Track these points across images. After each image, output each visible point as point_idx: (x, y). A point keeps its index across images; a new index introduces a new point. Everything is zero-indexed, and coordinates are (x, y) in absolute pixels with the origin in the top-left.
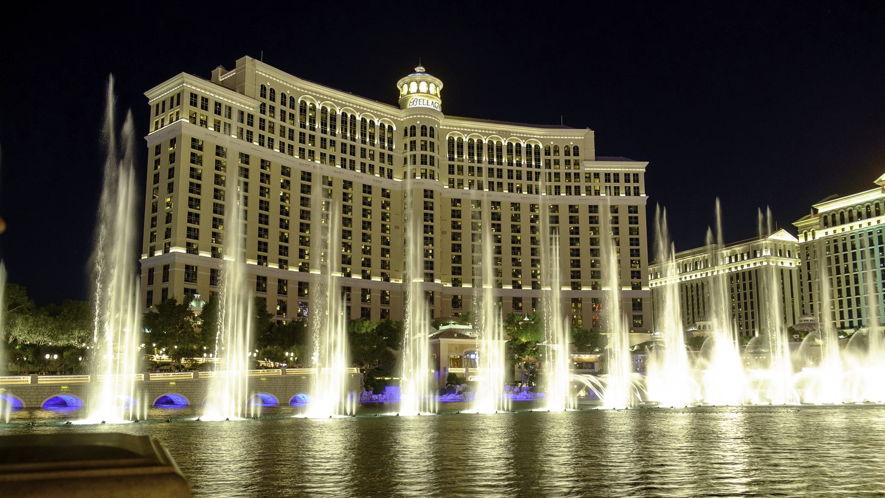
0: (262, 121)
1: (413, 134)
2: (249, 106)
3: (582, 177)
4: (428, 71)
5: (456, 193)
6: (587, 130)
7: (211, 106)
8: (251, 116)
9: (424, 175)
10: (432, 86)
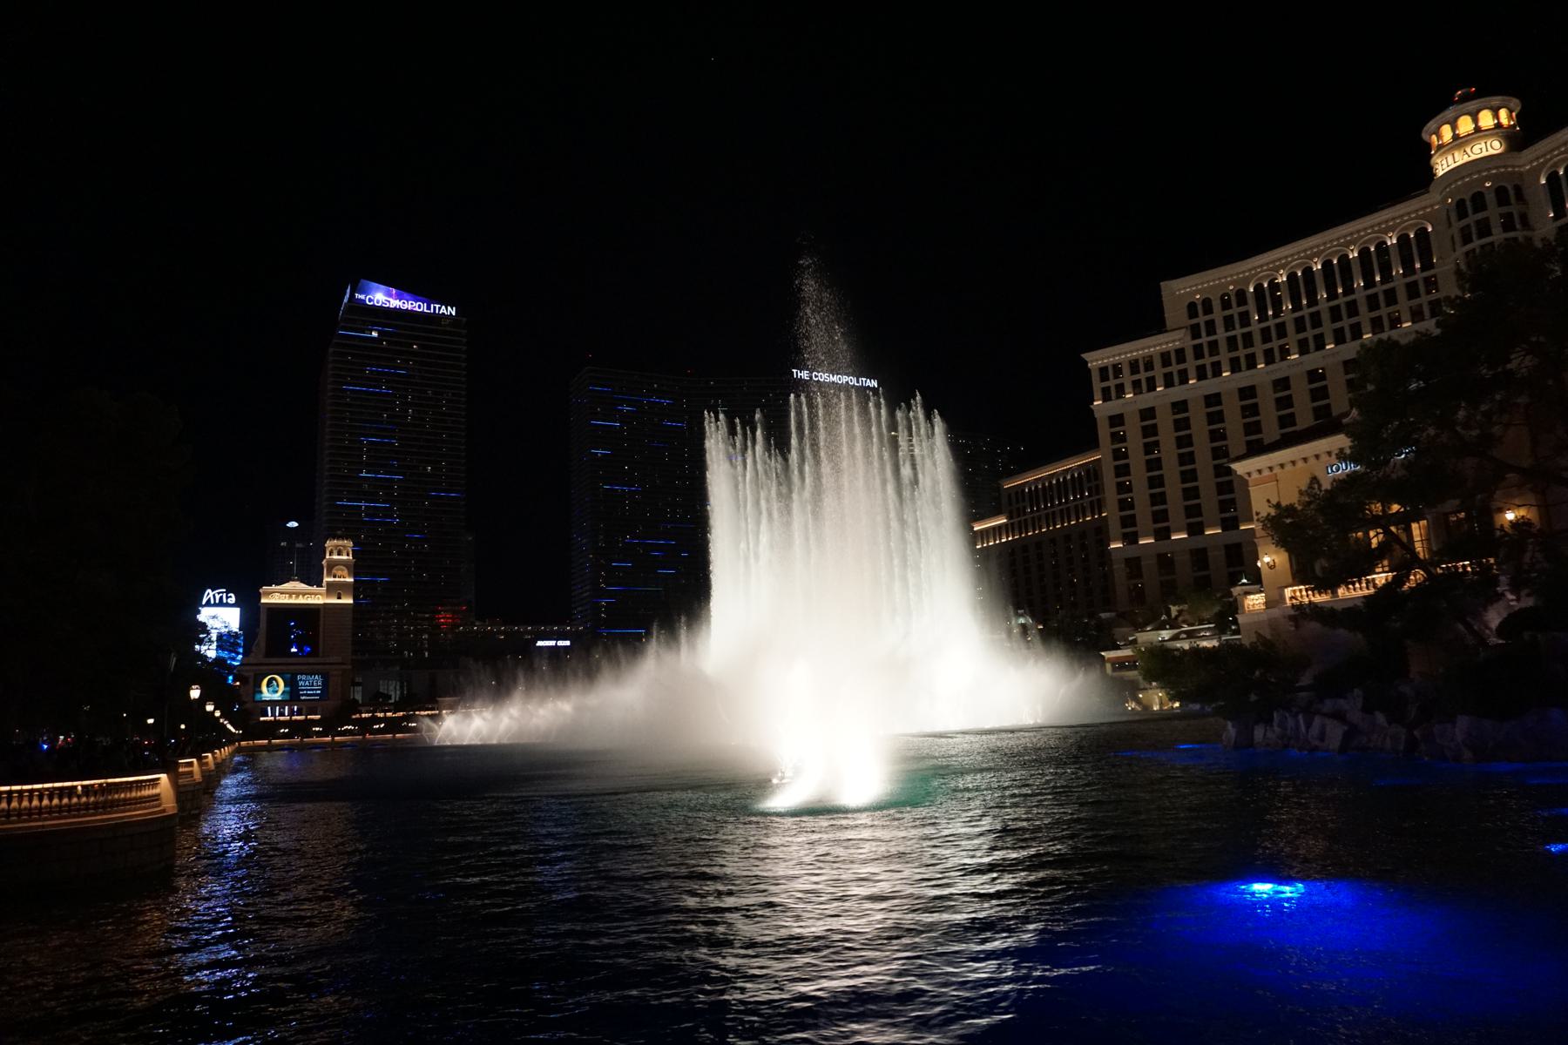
8: (1180, 353)
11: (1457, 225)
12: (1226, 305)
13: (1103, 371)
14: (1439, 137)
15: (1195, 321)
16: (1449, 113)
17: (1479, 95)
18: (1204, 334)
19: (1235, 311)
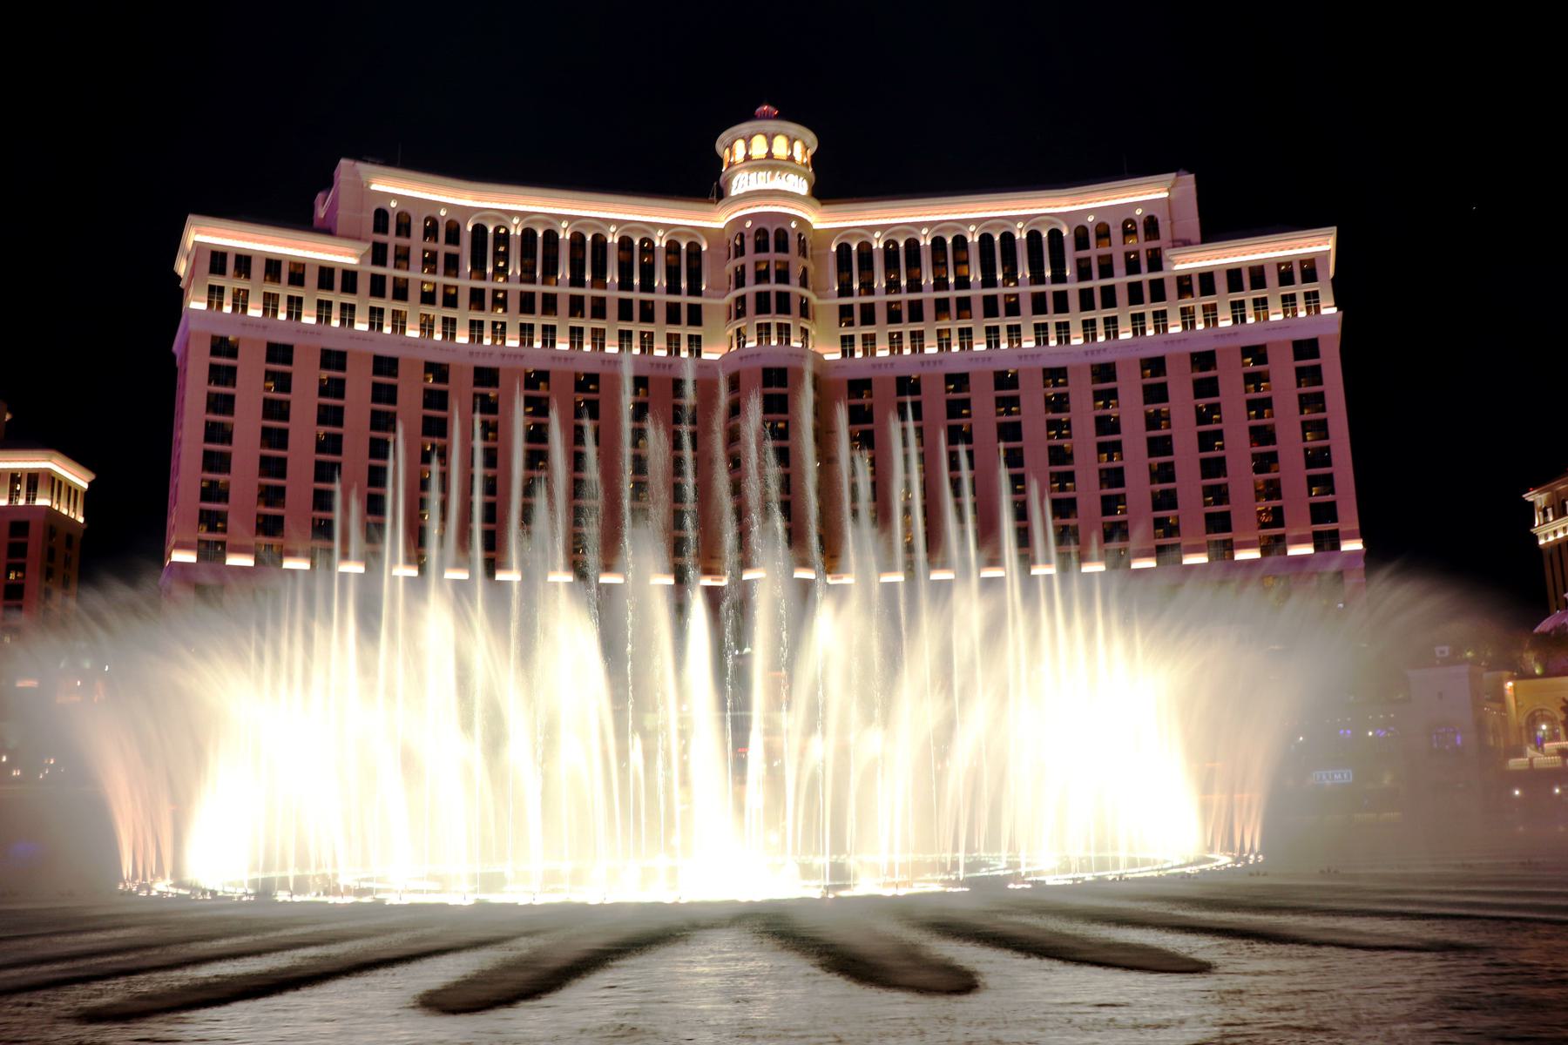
1: (740, 251)
3: (1171, 290)
6: (1172, 176)
7: (258, 269)
8: (350, 280)
11: (750, 259)
12: (431, 231)
13: (218, 261)
14: (748, 147)
15: (381, 238)
17: (779, 117)
19: (442, 248)
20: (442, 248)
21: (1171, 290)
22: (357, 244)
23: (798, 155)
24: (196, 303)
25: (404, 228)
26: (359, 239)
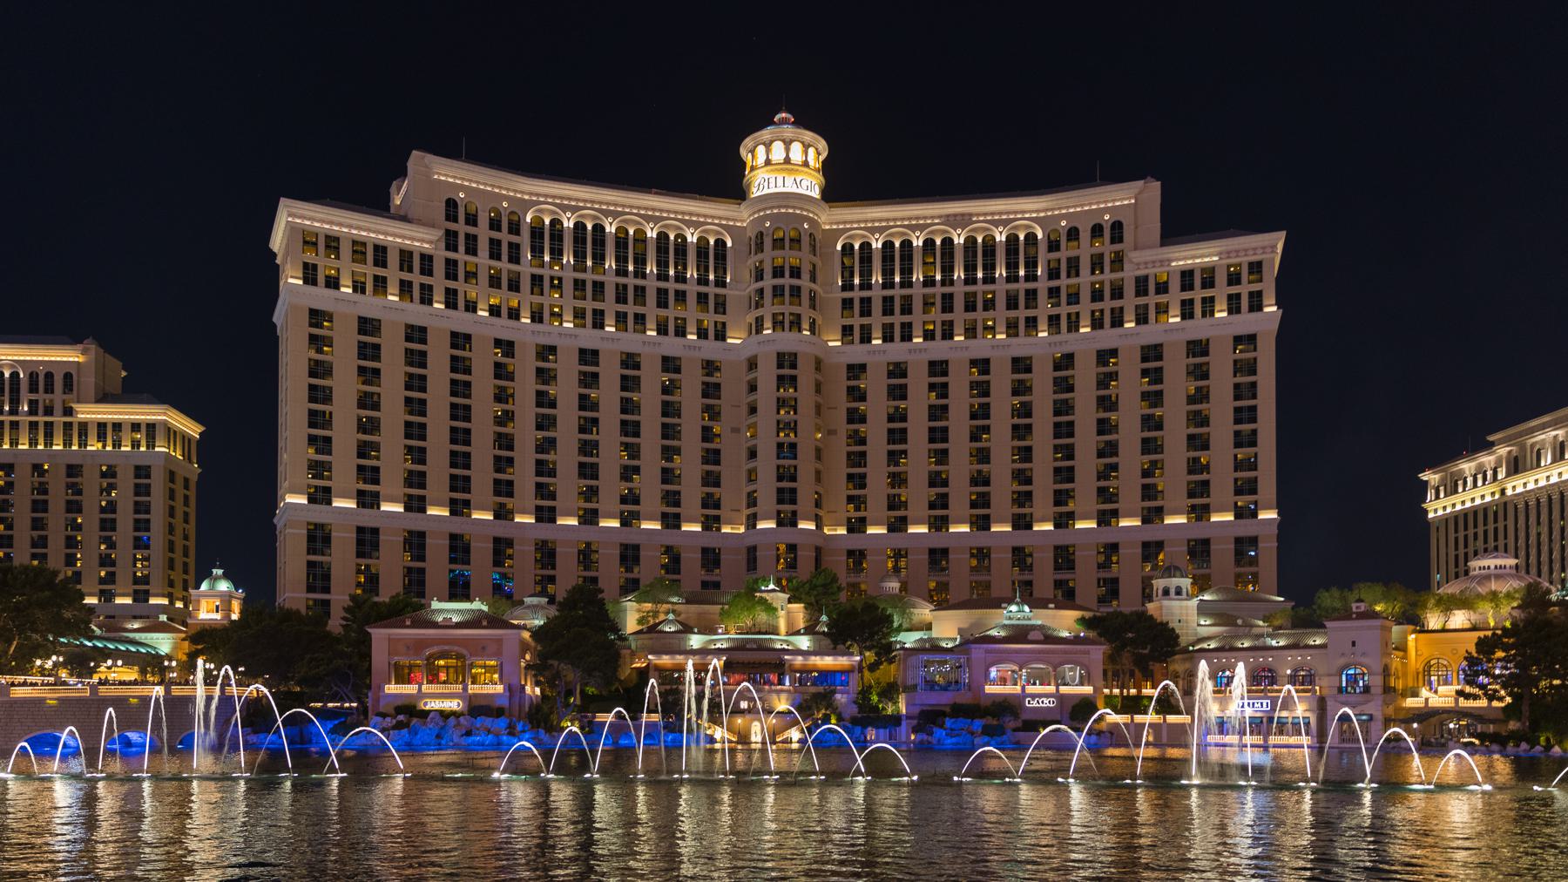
0: (451, 266)
1: (760, 247)
2: (422, 241)
3: (1129, 289)
4: (801, 122)
5: (857, 353)
7: (346, 250)
8: (427, 259)
9: (778, 324)
10: (796, 148)
12: (495, 225)
13: (309, 240)
15: (452, 226)
16: (766, 134)
18: (462, 248)
20: (504, 236)
21: (1129, 289)
22: (432, 231)
23: (812, 163)
24: (292, 279)
25: (472, 220)
26: (433, 226)
